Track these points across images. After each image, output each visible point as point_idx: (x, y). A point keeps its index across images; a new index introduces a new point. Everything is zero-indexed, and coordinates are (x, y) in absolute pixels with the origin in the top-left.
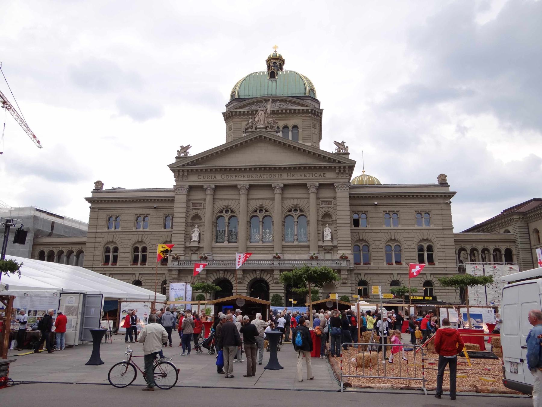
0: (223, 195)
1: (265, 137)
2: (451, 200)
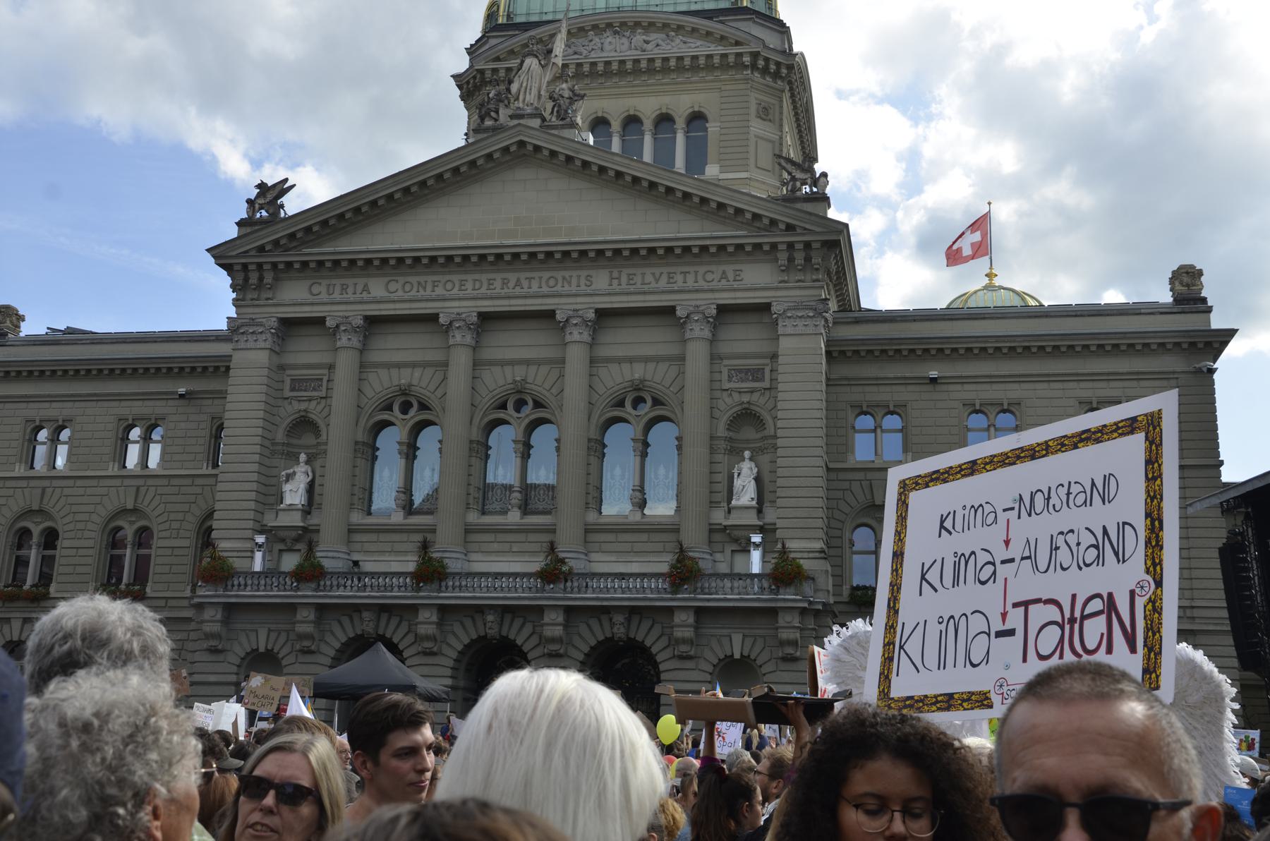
0: (395, 347)
1: (537, 149)
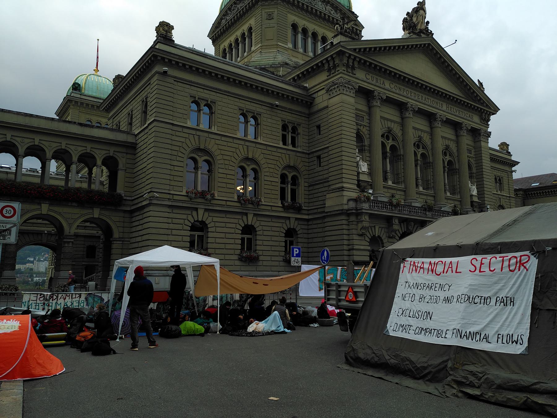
2: (513, 169)
